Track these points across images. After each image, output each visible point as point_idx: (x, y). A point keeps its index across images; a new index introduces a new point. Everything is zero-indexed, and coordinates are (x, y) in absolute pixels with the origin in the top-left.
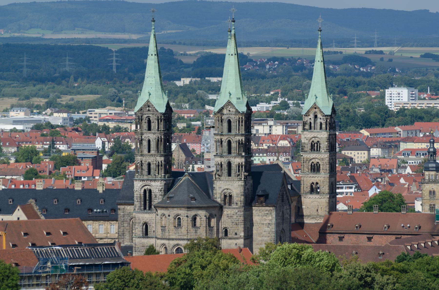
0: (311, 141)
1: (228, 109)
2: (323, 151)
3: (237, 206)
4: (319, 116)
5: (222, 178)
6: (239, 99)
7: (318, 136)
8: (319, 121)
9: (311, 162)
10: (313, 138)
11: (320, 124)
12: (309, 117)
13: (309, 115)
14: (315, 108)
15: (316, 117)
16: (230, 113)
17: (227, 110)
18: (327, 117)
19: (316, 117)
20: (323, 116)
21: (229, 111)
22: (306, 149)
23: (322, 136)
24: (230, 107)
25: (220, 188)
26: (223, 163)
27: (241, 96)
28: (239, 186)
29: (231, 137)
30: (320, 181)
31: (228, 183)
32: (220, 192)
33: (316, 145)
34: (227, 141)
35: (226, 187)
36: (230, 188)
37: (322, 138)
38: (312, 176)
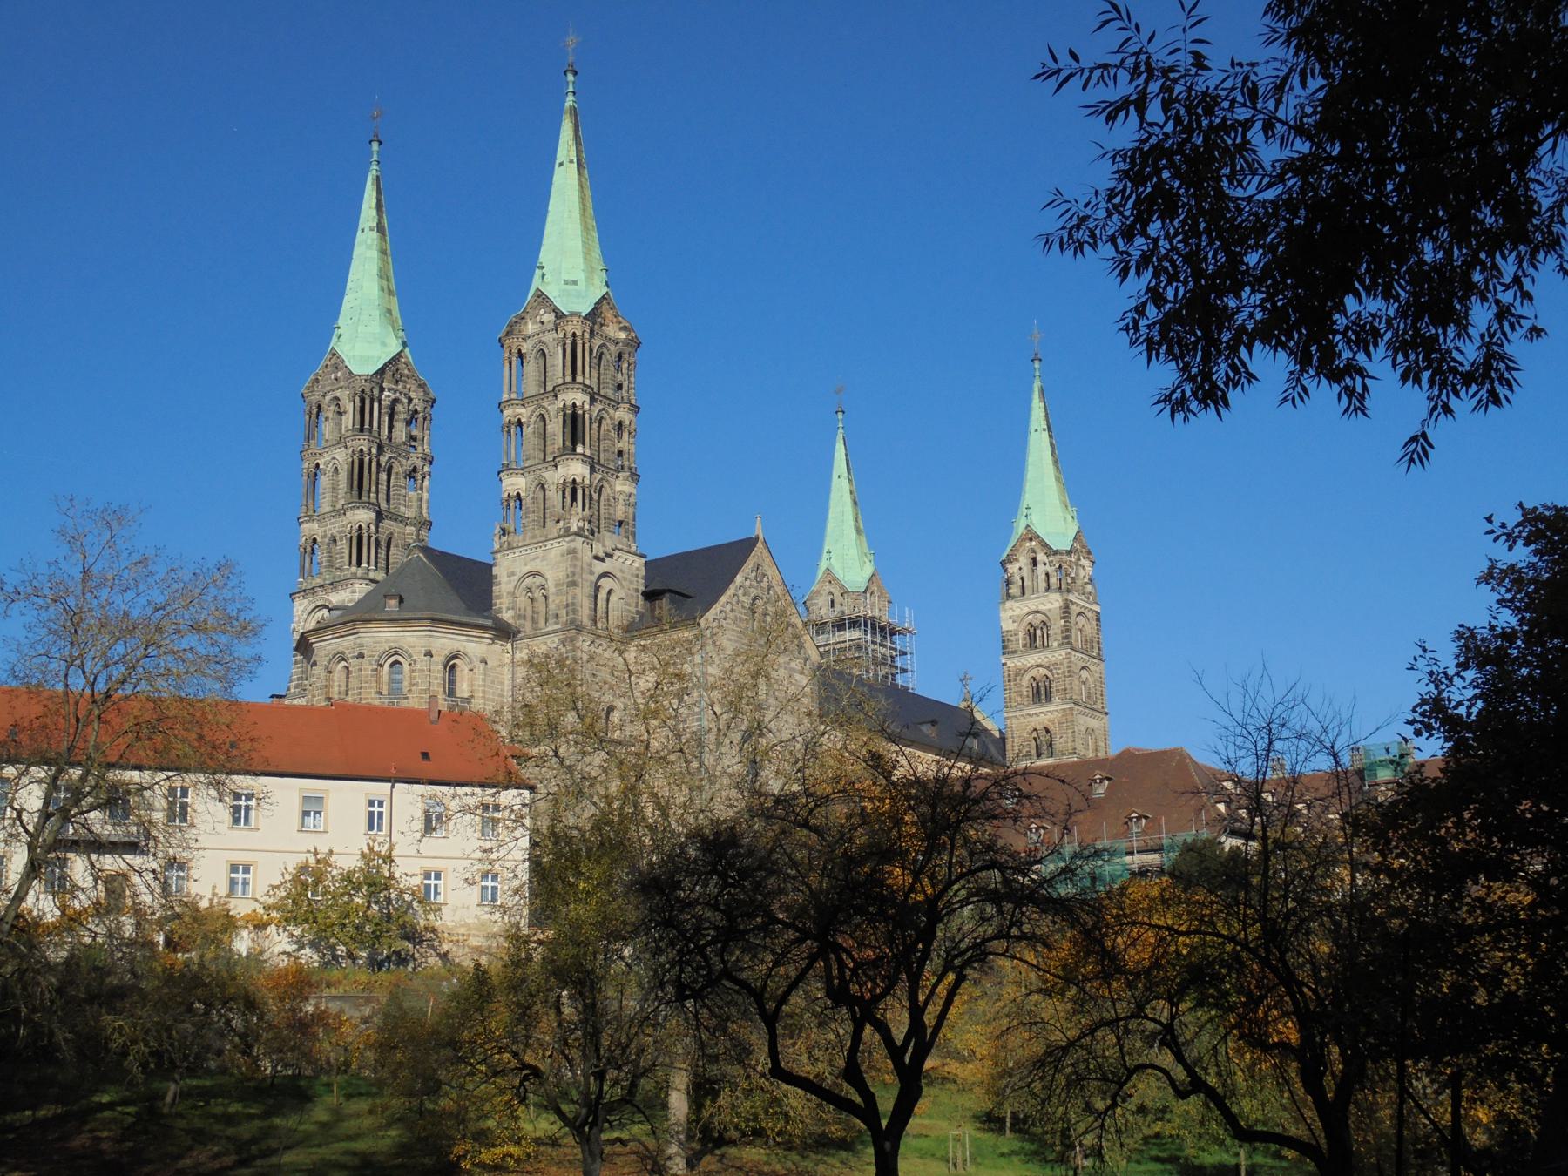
0: (1025, 623)
1: (538, 319)
2: (1055, 644)
3: (557, 623)
4: (1041, 557)
5: (516, 539)
6: (575, 283)
7: (1041, 608)
8: (1041, 569)
9: (1027, 677)
10: (1028, 614)
11: (1044, 576)
12: (1017, 566)
13: (1017, 560)
14: (1031, 540)
15: (1034, 562)
16: (544, 327)
17: (535, 323)
18: (1059, 557)
19: (1034, 562)
20: (1048, 555)
21: (542, 323)
22: (1011, 647)
23: (1049, 606)
24: (542, 311)
25: (513, 574)
26: (522, 494)
27: (580, 276)
28: (563, 555)
29: (546, 404)
30: (1053, 721)
31: (533, 553)
32: (511, 587)
33: (1039, 632)
34: (534, 418)
35: (528, 569)
36: (538, 569)
37: (1050, 610)
38: (1031, 712)
